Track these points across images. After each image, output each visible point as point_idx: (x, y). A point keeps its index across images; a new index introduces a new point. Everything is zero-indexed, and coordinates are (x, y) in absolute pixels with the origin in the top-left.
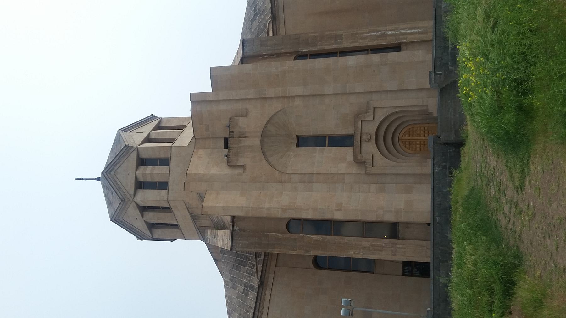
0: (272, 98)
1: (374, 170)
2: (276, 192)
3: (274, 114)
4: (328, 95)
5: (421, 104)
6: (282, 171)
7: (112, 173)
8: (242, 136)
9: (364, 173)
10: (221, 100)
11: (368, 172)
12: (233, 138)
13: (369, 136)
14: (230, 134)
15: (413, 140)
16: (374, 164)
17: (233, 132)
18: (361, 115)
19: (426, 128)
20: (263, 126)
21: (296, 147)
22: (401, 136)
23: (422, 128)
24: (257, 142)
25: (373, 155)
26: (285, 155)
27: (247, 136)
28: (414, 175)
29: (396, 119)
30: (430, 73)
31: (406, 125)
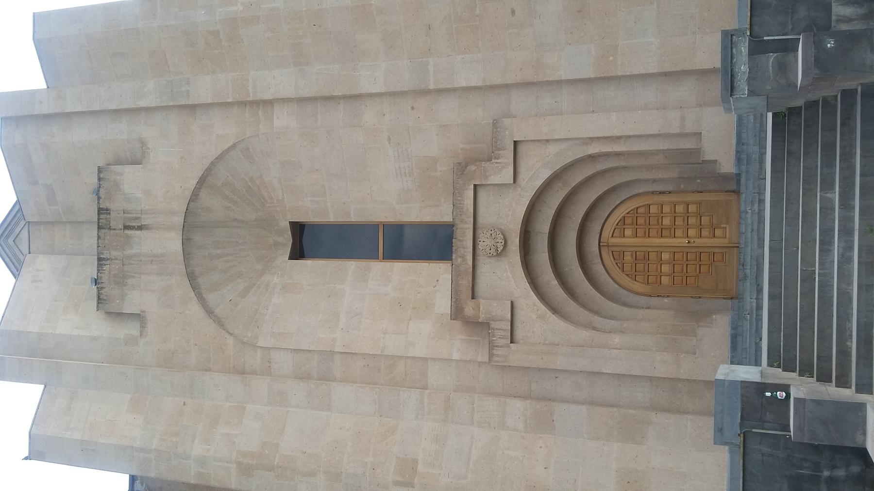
0: (207, 107)
1: (516, 356)
2: (228, 404)
3: (217, 158)
4: (371, 96)
5: (675, 130)
6: (245, 339)
7: (11, 241)
8: (134, 226)
9: (486, 359)
10: (73, 113)
11: (496, 359)
12: (110, 228)
13: (500, 237)
14: (102, 216)
15: (645, 249)
16: (519, 334)
17: (107, 211)
18: (473, 168)
19: (692, 208)
20: (188, 194)
21: (291, 258)
22: (607, 232)
23: (680, 209)
24: (173, 243)
25: (512, 303)
26: (254, 284)
27: (145, 225)
28: (650, 379)
29: (588, 181)
30: (729, 39)
31: (624, 195)
